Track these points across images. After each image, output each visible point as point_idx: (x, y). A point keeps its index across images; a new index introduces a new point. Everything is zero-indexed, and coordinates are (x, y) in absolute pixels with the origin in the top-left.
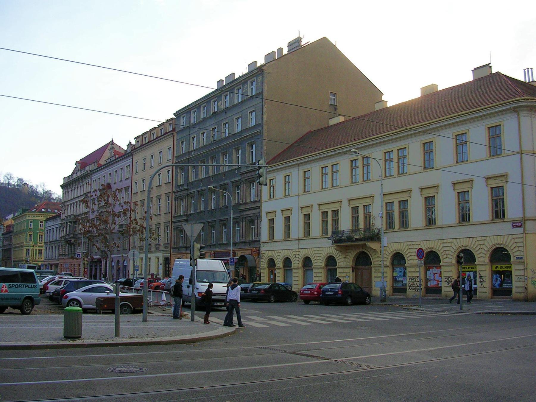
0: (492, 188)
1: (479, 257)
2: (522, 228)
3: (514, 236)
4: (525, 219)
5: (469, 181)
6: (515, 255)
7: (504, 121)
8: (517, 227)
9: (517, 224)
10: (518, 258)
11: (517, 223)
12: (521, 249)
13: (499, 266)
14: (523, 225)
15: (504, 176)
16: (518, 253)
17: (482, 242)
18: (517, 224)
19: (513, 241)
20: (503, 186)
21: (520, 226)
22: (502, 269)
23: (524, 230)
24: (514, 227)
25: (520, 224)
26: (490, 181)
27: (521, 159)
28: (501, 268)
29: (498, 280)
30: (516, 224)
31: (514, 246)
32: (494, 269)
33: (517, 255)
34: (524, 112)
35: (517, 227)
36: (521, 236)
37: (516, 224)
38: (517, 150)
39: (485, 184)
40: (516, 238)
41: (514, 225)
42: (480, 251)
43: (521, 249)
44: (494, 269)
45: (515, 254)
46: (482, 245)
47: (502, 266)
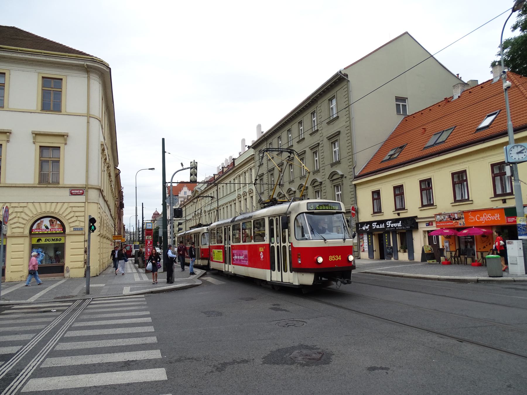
0: (40, 147)
1: (13, 228)
2: (85, 196)
3: (71, 205)
4: (89, 186)
5: (6, 133)
6: (71, 226)
7: (68, 77)
8: (77, 194)
9: (78, 191)
10: (75, 229)
11: (77, 190)
12: (79, 218)
13: (43, 239)
14: (85, 192)
15: (63, 136)
16: (77, 223)
17: (20, 210)
18: (78, 191)
19: (69, 210)
20: (60, 147)
21: (82, 194)
22: (48, 242)
23: (87, 199)
24: (72, 194)
25: (81, 192)
26: (39, 139)
27: (88, 122)
28: (45, 241)
29: (41, 256)
30: (76, 191)
31: (72, 214)
32: (34, 241)
33: (76, 226)
34: (95, 75)
35: (77, 194)
36: (83, 205)
37: (76, 191)
38: (84, 111)
39: (32, 140)
40: (75, 207)
41: (73, 192)
42: (15, 220)
43: (79, 218)
44: (34, 241)
45: (72, 225)
46: (19, 214)
47: (48, 238)
